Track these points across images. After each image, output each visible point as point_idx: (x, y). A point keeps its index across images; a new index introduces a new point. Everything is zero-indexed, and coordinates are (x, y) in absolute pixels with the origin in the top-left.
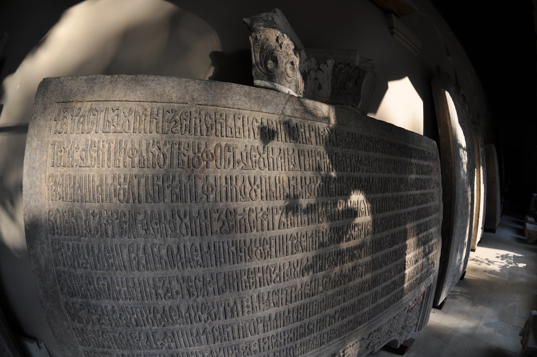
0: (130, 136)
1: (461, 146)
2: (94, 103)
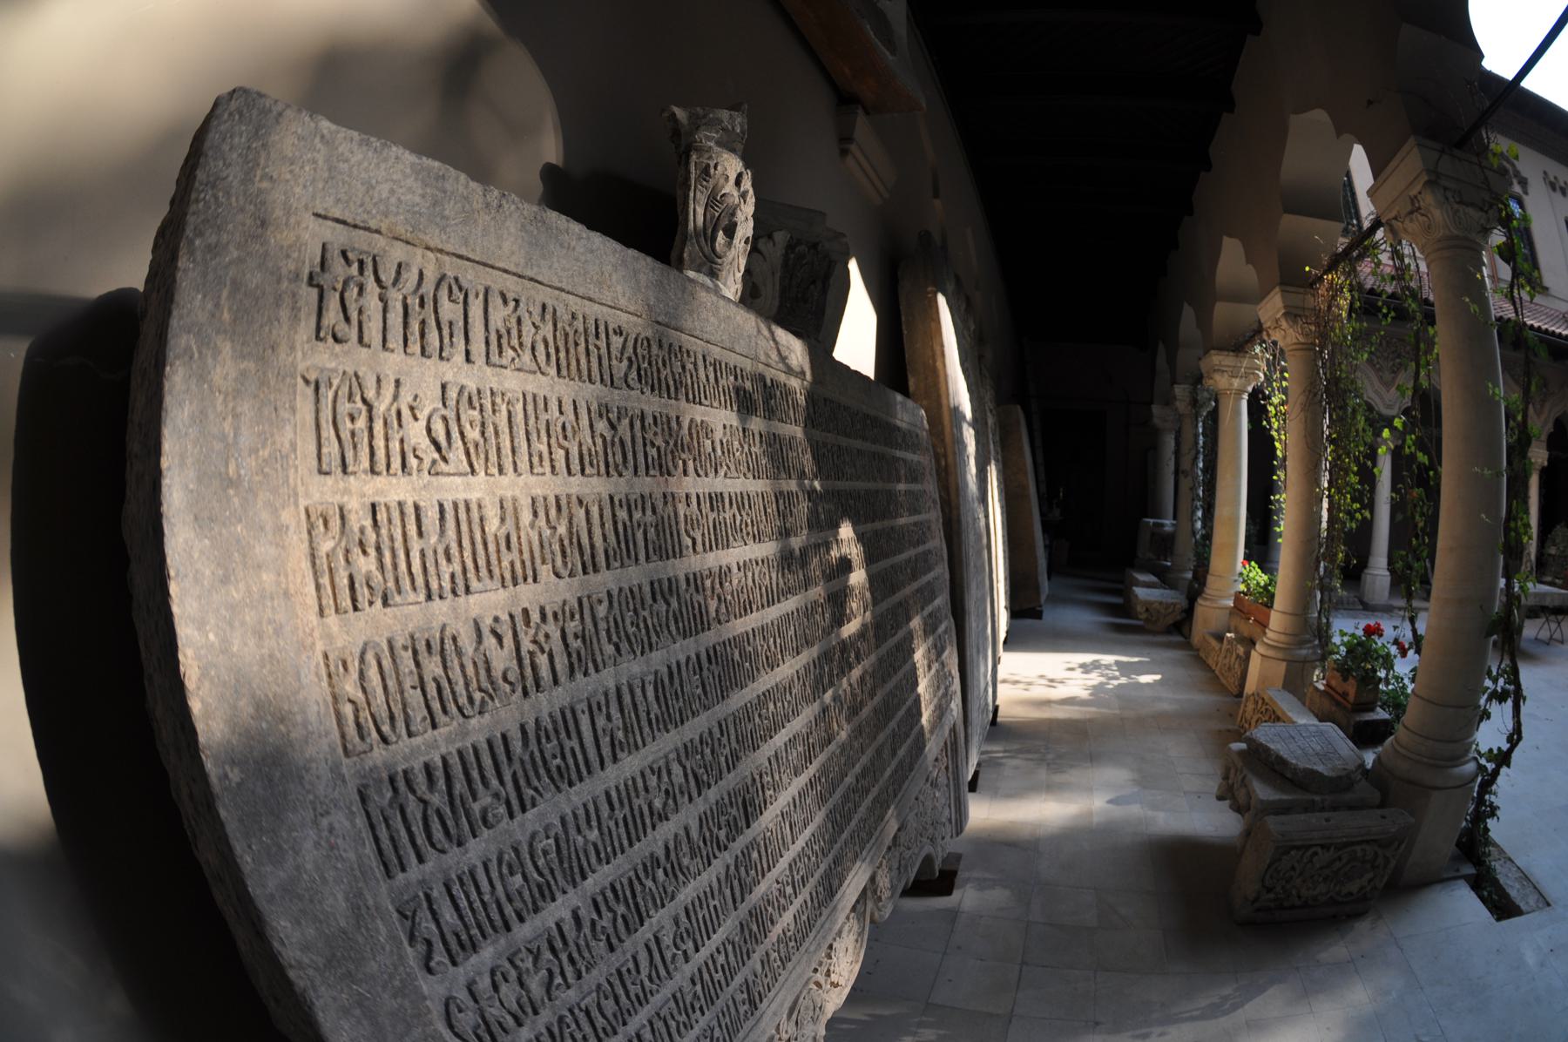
2: (447, 258)
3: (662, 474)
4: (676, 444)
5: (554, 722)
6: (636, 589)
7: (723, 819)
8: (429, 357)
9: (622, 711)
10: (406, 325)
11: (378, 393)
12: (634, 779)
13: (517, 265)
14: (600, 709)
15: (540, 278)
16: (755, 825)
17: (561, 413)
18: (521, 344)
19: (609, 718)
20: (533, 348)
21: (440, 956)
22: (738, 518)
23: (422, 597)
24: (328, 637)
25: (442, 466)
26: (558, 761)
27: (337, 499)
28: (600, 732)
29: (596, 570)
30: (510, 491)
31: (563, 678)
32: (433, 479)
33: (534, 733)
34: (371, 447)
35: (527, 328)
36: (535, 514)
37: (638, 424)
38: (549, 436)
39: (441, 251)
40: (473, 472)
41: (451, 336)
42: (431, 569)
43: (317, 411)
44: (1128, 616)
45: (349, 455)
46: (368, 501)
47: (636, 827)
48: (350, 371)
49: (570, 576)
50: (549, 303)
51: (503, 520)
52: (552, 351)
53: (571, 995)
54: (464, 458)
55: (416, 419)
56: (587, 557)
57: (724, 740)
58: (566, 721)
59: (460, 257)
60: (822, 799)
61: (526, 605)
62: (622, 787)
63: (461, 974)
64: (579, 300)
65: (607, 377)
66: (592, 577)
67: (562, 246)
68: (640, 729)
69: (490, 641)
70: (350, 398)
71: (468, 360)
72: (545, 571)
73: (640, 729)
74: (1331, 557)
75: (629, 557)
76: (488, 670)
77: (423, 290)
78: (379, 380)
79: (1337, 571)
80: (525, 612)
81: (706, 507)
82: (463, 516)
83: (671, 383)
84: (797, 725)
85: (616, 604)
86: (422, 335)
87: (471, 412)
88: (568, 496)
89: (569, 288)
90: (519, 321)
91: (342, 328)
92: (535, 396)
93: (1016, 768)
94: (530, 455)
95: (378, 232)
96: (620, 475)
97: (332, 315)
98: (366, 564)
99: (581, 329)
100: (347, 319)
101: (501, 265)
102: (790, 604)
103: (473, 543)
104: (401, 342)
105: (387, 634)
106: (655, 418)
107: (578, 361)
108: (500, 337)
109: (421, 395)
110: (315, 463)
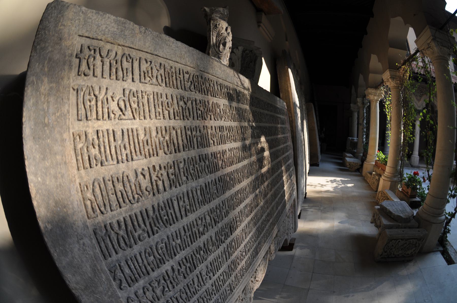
0: (164, 90)
1: (297, 105)
2: (126, 48)
3: (203, 120)
4: (207, 110)
5: (164, 204)
6: (194, 158)
7: (223, 233)
8: (119, 80)
9: (189, 199)
10: (110, 69)
11: (100, 92)
12: (193, 222)
13: (151, 51)
14: (181, 199)
15: (159, 55)
16: (234, 234)
17: (167, 99)
18: (152, 76)
19: (184, 202)
20: (157, 77)
21: (124, 284)
22: (229, 134)
23: (115, 162)
24: (81, 177)
25: (123, 117)
26: (166, 217)
27: (84, 129)
28: (181, 207)
29: (179, 151)
30: (148, 125)
31: (167, 189)
32: (120, 121)
33: (157, 209)
34: (97, 111)
35: (155, 71)
36: (157, 133)
37: (194, 103)
38: (162, 106)
39: (124, 46)
40: (134, 118)
41: (127, 73)
42: (119, 152)
43: (77, 99)
44: (345, 167)
45: (89, 114)
46: (95, 129)
47: (193, 238)
48: (90, 85)
49: (170, 154)
50: (163, 63)
51: (145, 135)
52: (164, 78)
53: (171, 293)
54: (131, 114)
55: (113, 101)
56: (176, 147)
57: (224, 207)
58: (169, 203)
59: (131, 48)
60: (255, 224)
61: (154, 164)
62: (189, 225)
63: (133, 289)
64: (173, 62)
65: (183, 87)
66: (178, 154)
67: (167, 45)
68: (195, 205)
69: (141, 177)
70: (89, 94)
71: (133, 81)
72: (161, 152)
73: (195, 205)
74: (404, 151)
75: (191, 147)
76: (140, 187)
77: (117, 58)
78: (100, 88)
79: (406, 155)
80: (154, 166)
81: (218, 131)
82: (130, 134)
83: (206, 90)
84: (247, 201)
85: (186, 163)
86: (116, 73)
87: (134, 98)
88: (169, 127)
89: (170, 58)
90: (152, 68)
91: (87, 71)
92: (157, 93)
93: (312, 212)
94: (156, 113)
95: (101, 40)
96: (188, 120)
97: (84, 67)
98: (94, 152)
99: (174, 71)
100: (89, 68)
101: (145, 50)
102: (245, 162)
103: (134, 143)
104: (109, 75)
105: (102, 176)
106: (200, 101)
107: (173, 82)
108: (145, 73)
109: (115, 93)
110: (76, 117)
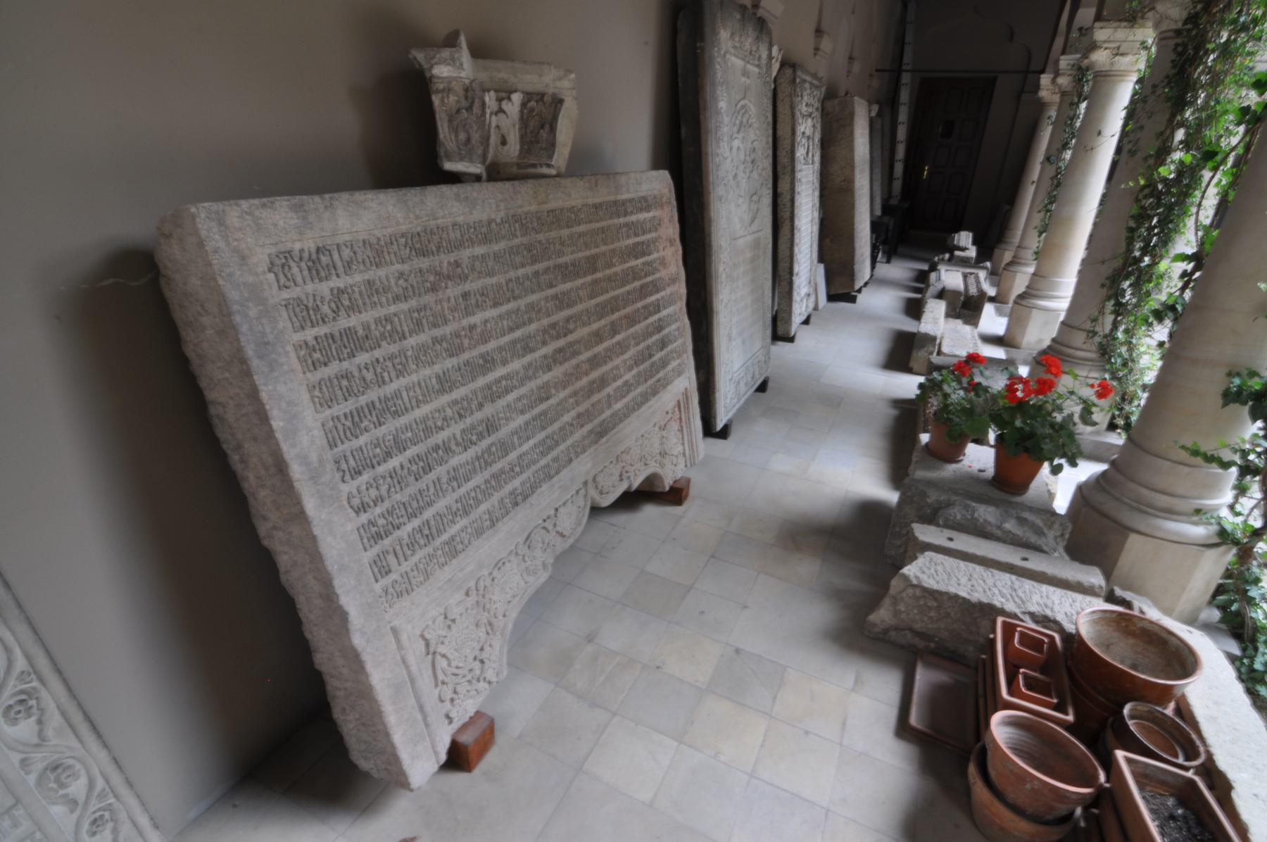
21: (348, 477)
47: (428, 432)
53: (398, 497)
63: (355, 483)
91: (288, 284)
98: (317, 355)
